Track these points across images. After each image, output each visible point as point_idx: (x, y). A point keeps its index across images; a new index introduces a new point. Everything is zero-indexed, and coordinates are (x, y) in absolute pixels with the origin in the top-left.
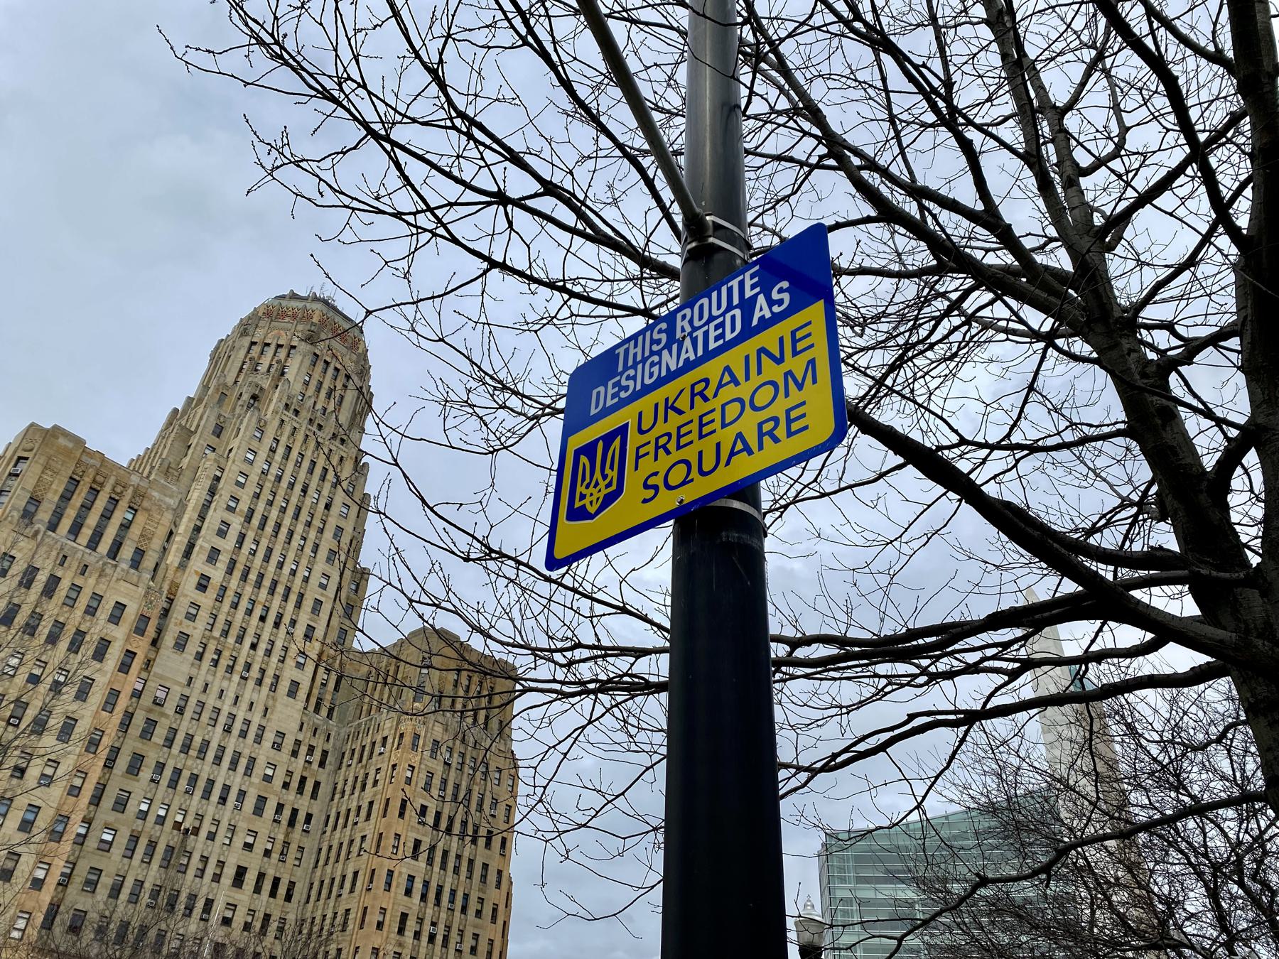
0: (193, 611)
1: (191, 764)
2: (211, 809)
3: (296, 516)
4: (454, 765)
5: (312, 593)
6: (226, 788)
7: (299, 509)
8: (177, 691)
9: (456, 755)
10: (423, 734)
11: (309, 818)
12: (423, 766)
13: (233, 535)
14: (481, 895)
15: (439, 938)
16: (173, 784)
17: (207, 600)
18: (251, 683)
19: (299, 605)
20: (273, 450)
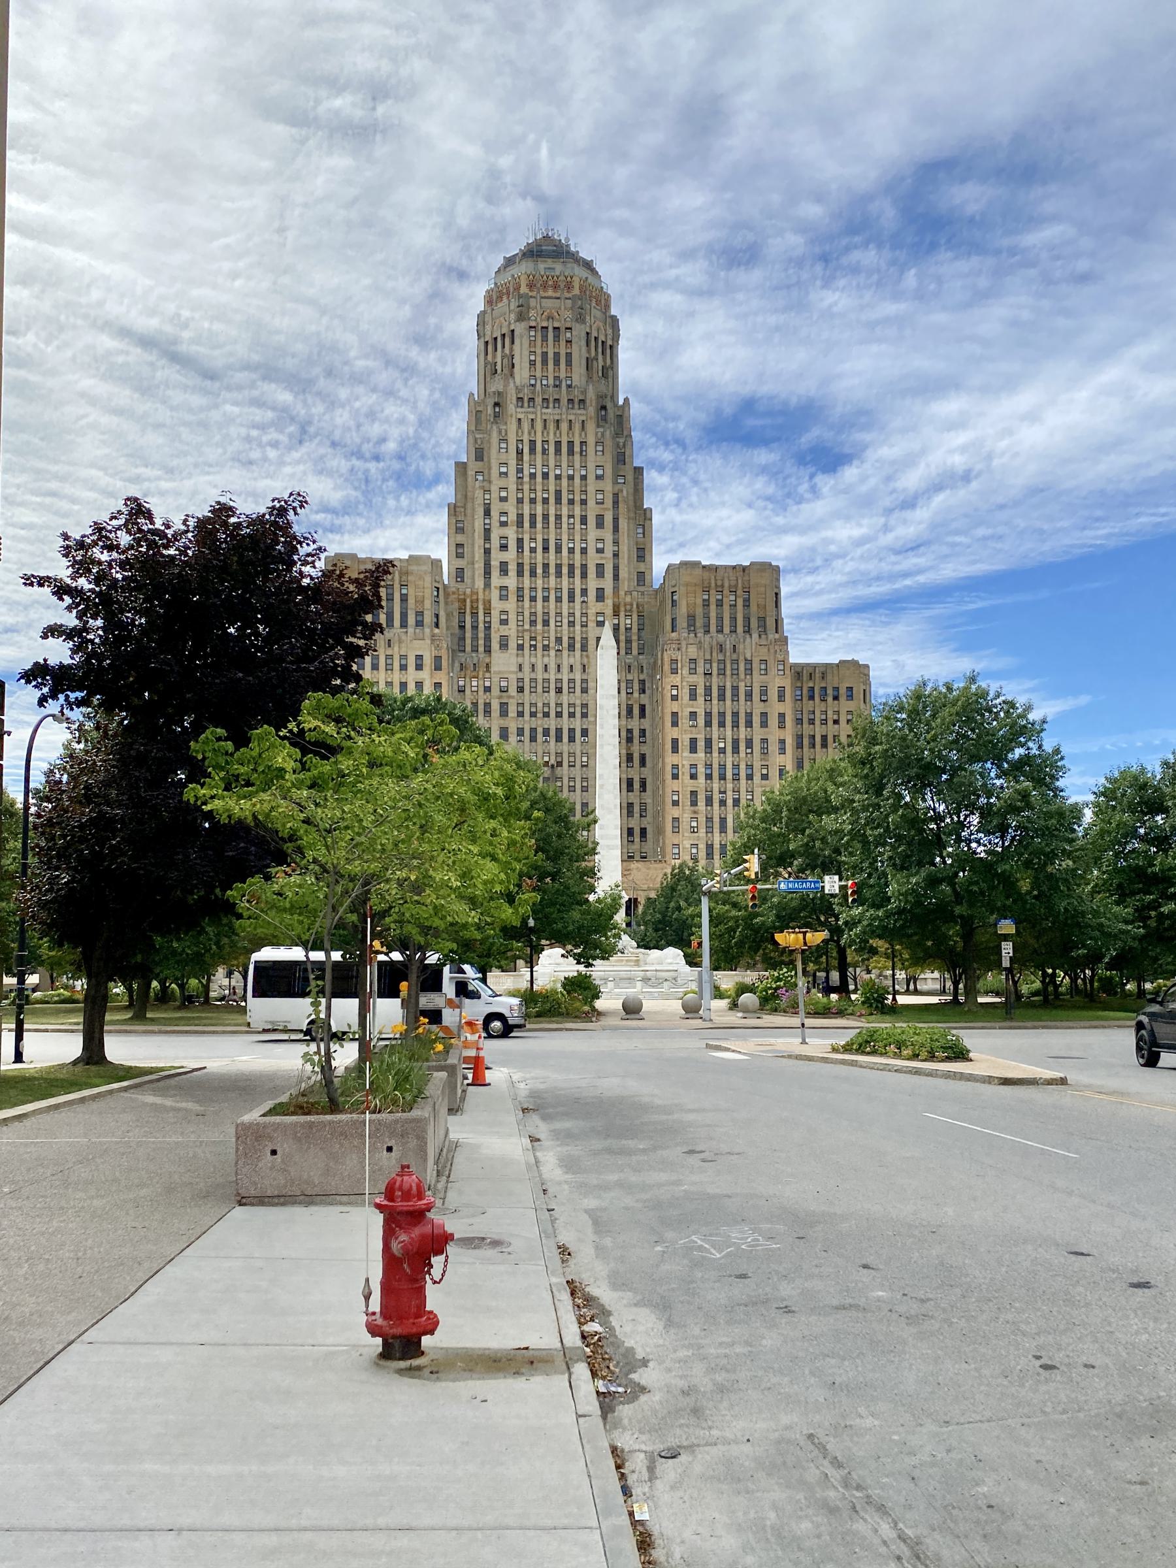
0: (504, 617)
1: (540, 723)
2: (565, 746)
3: (558, 500)
4: (715, 672)
5: (593, 559)
6: (572, 731)
7: (558, 494)
8: (513, 678)
9: (715, 665)
10: (679, 658)
11: (643, 732)
12: (684, 684)
13: (512, 545)
14: (764, 763)
15: (730, 802)
16: (533, 739)
17: (511, 605)
18: (565, 653)
19: (584, 575)
20: (520, 453)
